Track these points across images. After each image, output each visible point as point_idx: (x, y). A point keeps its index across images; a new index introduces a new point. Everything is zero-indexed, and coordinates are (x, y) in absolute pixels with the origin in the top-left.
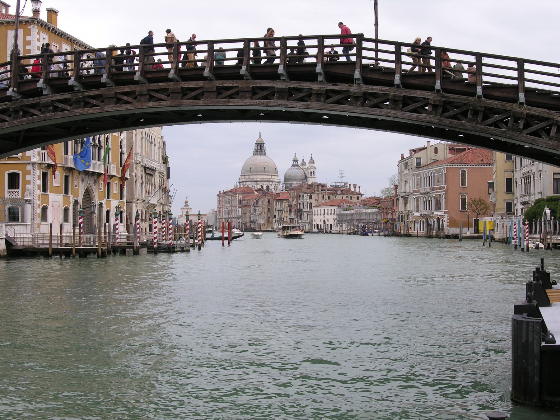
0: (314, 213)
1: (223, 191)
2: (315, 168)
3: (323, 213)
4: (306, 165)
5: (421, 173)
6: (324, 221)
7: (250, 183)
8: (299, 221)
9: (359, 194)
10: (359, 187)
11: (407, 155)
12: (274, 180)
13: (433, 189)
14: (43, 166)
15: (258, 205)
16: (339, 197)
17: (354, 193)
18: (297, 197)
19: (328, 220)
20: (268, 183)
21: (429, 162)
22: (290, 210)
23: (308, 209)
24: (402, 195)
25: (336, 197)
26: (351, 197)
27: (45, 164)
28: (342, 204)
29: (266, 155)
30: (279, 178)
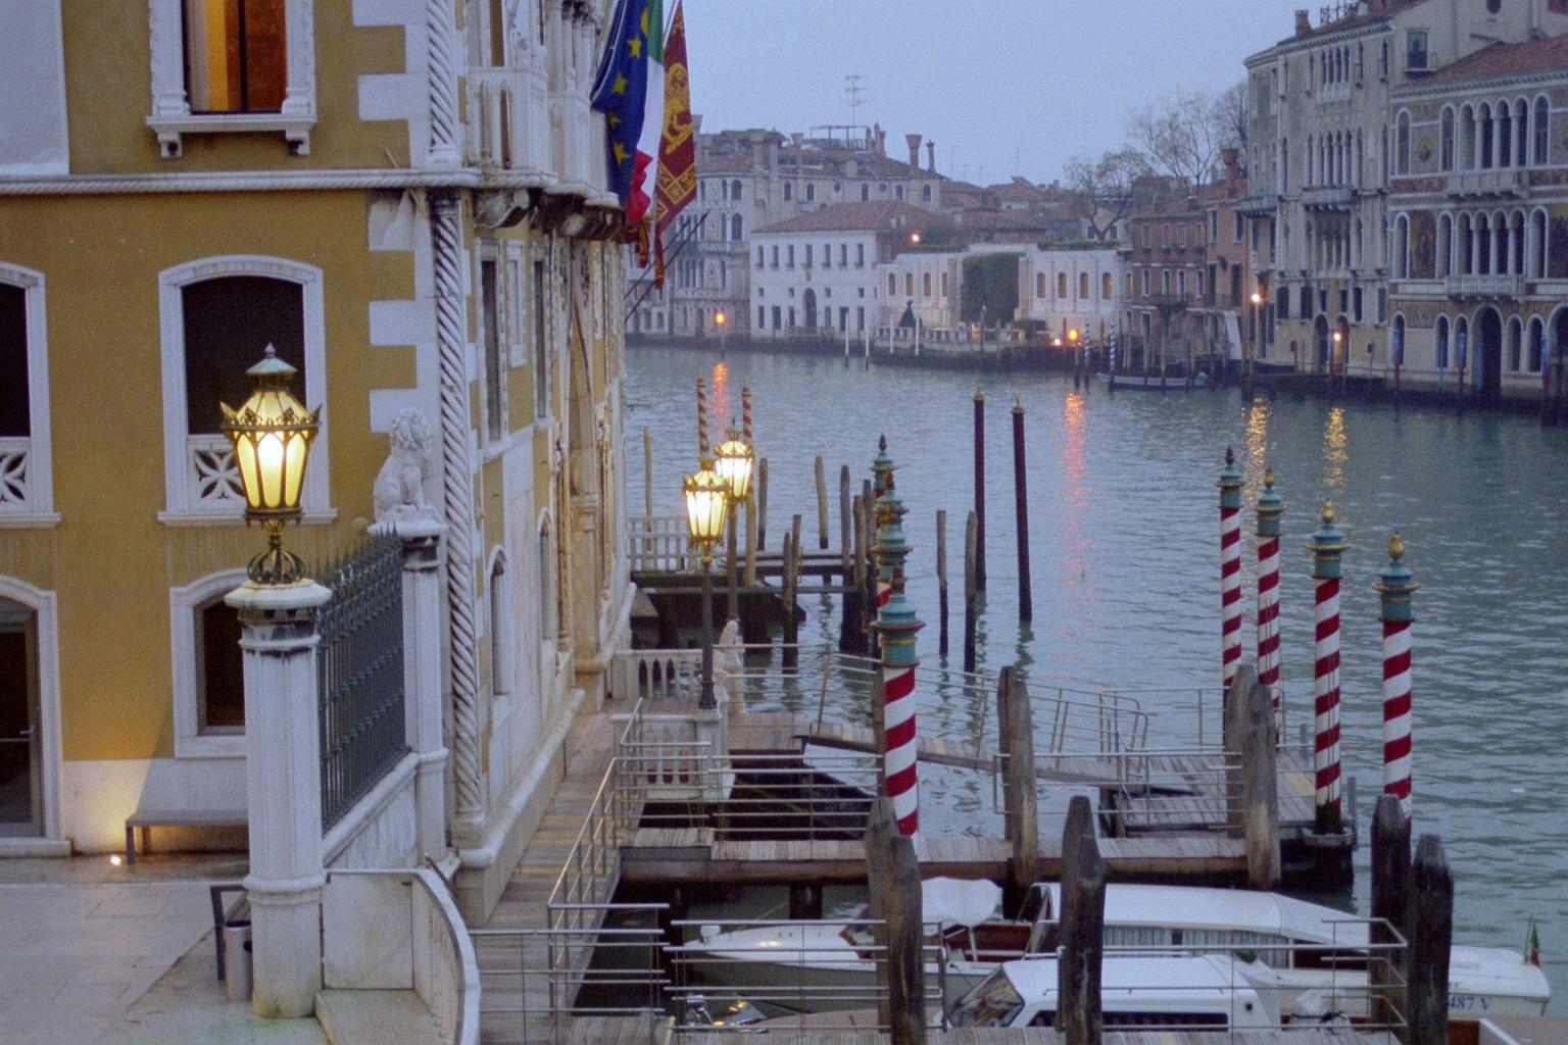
0: (754, 258)
3: (804, 261)
5: (1447, 100)
6: (810, 297)
8: (680, 293)
9: (931, 173)
10: (930, 145)
13: (1535, 178)
14: (498, 207)
16: (852, 192)
19: (828, 292)
21: (1467, 48)
24: (1309, 197)
26: (899, 190)
27: (510, 192)
28: (893, 222)
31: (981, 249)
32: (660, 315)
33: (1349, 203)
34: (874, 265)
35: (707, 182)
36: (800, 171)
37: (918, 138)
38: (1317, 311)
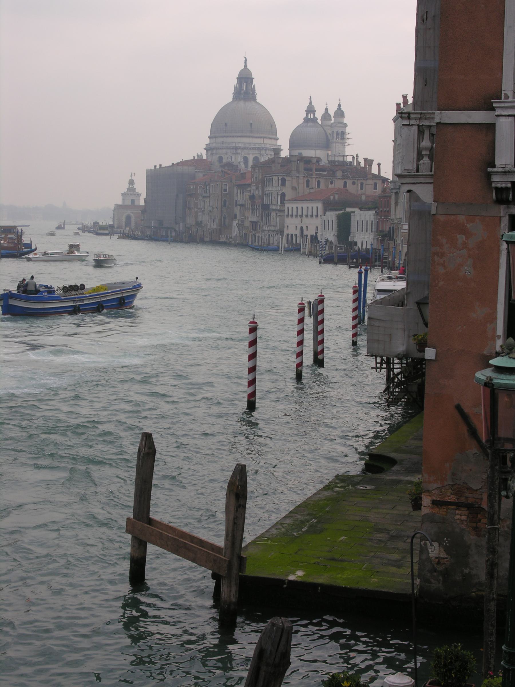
0: (286, 213)
1: (160, 165)
2: (346, 125)
4: (331, 120)
6: (302, 228)
7: (224, 151)
9: (378, 177)
10: (379, 165)
11: (402, 106)
12: (268, 146)
15: (208, 195)
16: (339, 184)
17: (369, 176)
18: (262, 181)
19: (307, 227)
20: (256, 152)
22: (253, 205)
23: (277, 205)
25: (332, 183)
26: (362, 184)
28: (332, 197)
29: (254, 98)
30: (279, 143)
31: (348, 210)
32: (258, 236)
33: (398, 189)
34: (321, 215)
35: (274, 177)
36: (314, 174)
37: (372, 161)
38: (395, 238)
